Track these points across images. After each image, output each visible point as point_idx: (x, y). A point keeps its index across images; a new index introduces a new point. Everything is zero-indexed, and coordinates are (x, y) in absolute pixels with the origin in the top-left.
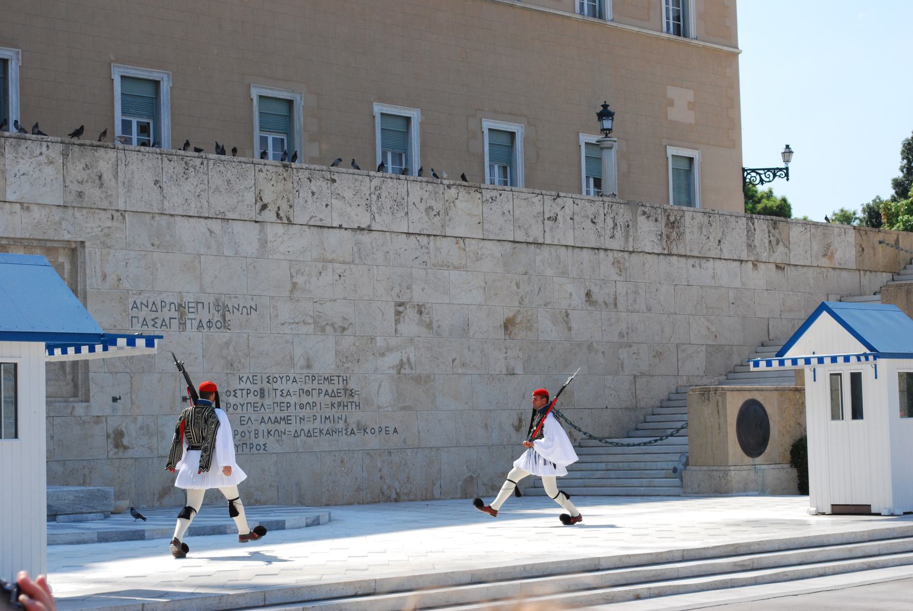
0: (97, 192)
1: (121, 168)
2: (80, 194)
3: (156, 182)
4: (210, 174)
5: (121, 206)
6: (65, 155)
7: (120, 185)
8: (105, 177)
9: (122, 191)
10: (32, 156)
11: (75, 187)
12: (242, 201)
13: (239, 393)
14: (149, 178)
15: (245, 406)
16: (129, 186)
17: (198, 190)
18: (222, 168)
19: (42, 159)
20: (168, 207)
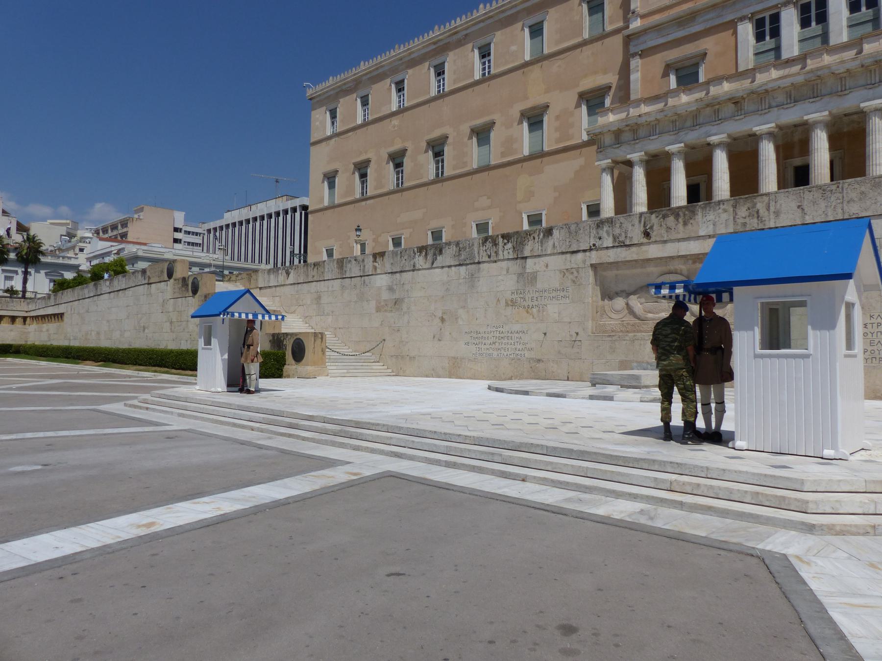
0: (755, 220)
1: (772, 204)
2: (744, 224)
3: (799, 207)
4: (845, 191)
5: (772, 225)
6: (735, 207)
7: (772, 213)
8: (761, 211)
9: (772, 216)
10: (714, 211)
11: (741, 221)
12: (875, 203)
13: (869, 326)
14: (794, 205)
15: (875, 335)
16: (777, 214)
17: (834, 204)
18: (856, 186)
19: (720, 211)
20: (808, 220)
